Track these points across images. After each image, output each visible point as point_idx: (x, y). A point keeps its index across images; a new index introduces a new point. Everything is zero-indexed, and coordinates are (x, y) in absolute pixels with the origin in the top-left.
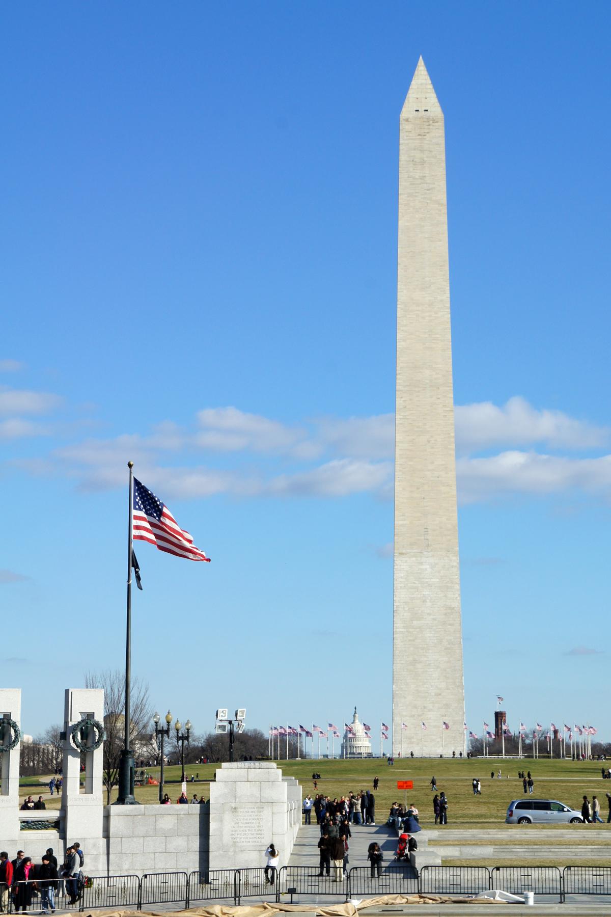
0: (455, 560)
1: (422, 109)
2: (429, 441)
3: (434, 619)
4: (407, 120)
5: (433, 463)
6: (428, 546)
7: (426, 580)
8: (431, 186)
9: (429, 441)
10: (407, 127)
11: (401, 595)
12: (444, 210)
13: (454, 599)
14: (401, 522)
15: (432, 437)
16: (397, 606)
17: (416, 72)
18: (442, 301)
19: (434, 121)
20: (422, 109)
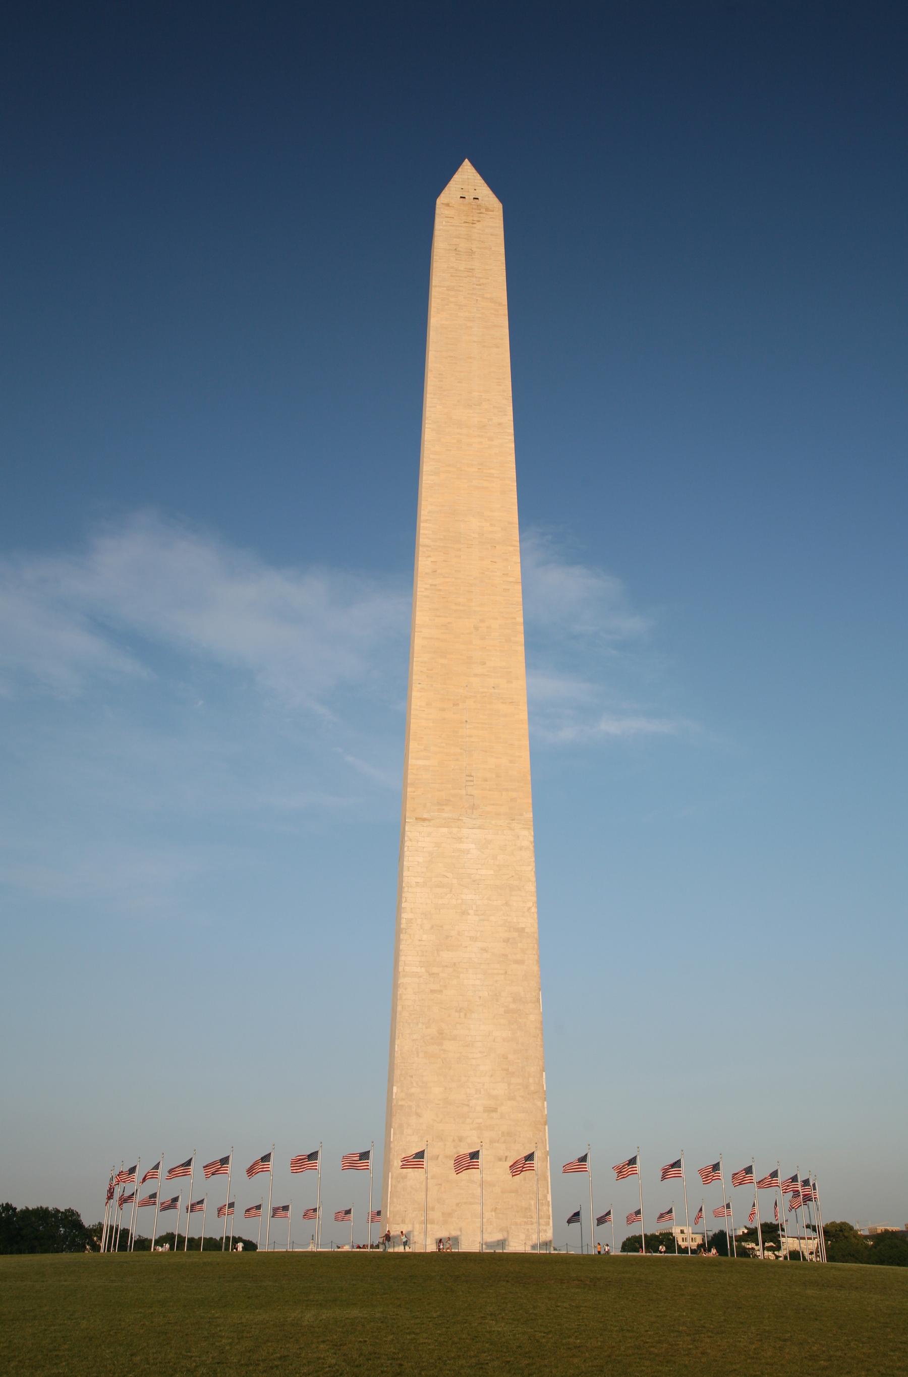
0: (527, 837)
1: (470, 197)
2: (476, 628)
3: (484, 950)
4: (448, 205)
5: (484, 664)
6: (474, 807)
7: (468, 874)
8: (482, 281)
9: (476, 628)
10: (446, 212)
11: (416, 899)
12: (505, 311)
13: (524, 910)
14: (421, 762)
15: (482, 621)
16: (410, 921)
17: (460, 170)
18: (500, 424)
19: (487, 210)
20: (470, 197)
